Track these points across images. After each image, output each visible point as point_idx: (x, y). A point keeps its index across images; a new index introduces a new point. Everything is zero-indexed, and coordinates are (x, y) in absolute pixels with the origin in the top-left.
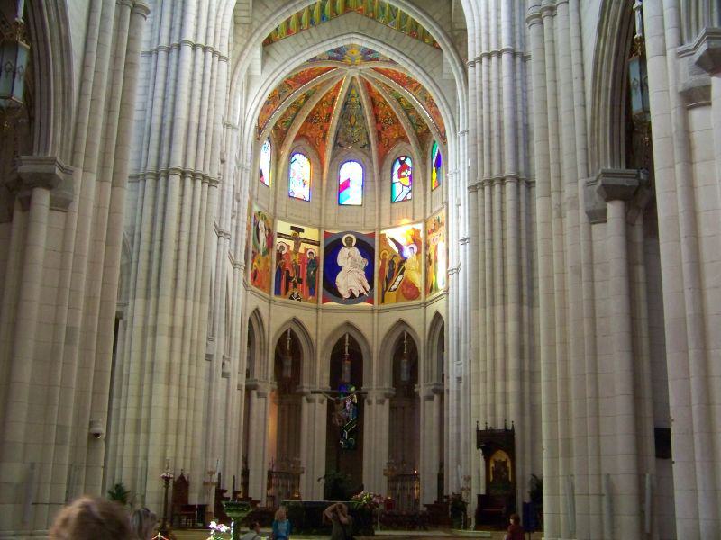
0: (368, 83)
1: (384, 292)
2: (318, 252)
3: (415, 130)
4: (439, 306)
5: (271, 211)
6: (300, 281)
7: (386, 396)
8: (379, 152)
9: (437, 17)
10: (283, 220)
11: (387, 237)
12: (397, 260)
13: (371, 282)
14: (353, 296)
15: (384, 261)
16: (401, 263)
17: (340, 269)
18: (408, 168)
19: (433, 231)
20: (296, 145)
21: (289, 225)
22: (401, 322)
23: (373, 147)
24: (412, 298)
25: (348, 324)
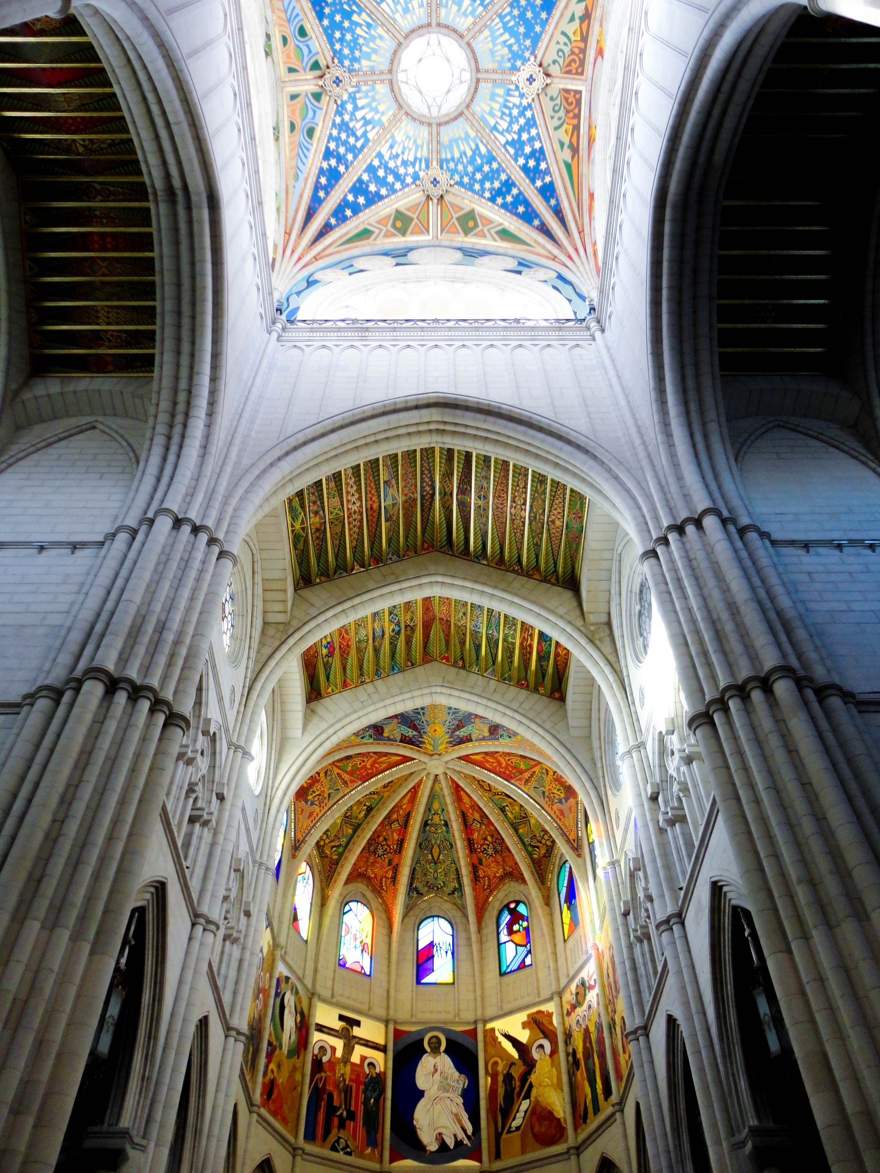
0: (458, 786)
1: (498, 1136)
3: (530, 854)
5: (308, 982)
8: (476, 898)
9: (561, 611)
10: (325, 1001)
11: (497, 1034)
12: (516, 1073)
14: (443, 1145)
16: (525, 1077)
17: (421, 1094)
18: (522, 917)
19: (574, 1007)
20: (350, 887)
21: (336, 1012)
23: (468, 890)
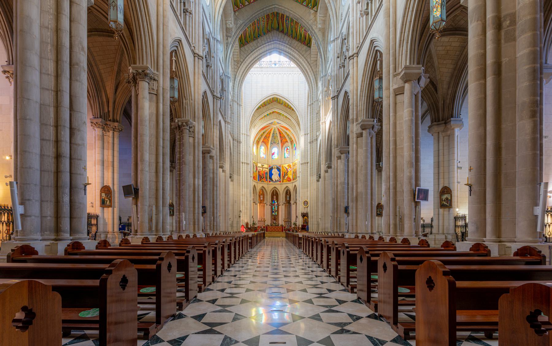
2: (267, 170)
4: (296, 183)
6: (264, 178)
7: (284, 203)
12: (286, 172)
13: (280, 177)
14: (276, 181)
15: (283, 172)
21: (261, 164)
22: (287, 187)
24: (289, 181)
25: (275, 187)
